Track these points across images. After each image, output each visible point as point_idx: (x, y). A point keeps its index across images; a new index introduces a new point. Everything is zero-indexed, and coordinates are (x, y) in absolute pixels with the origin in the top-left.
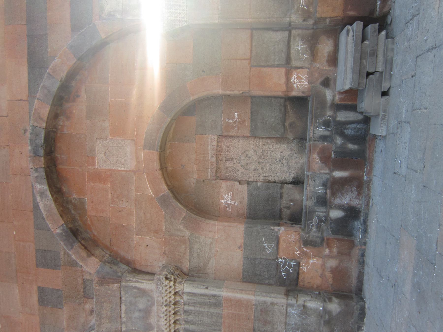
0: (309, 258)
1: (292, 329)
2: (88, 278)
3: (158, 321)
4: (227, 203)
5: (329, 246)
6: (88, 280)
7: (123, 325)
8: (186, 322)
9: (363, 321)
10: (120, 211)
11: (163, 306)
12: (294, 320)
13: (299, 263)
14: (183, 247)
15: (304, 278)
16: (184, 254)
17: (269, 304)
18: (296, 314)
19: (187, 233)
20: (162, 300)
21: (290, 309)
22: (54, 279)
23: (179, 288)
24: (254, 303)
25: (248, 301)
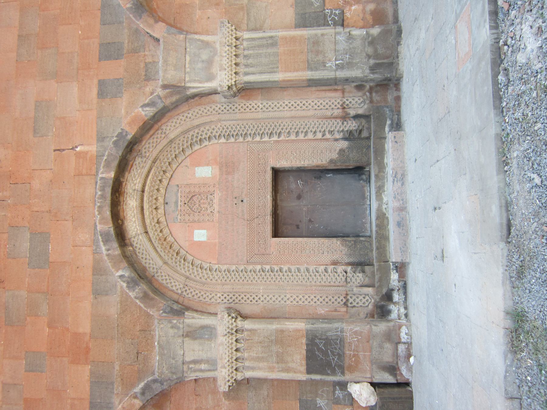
0: (351, 6)
1: (341, 54)
2: (150, 60)
3: (221, 60)
6: (150, 63)
7: (187, 75)
8: (245, 65)
9: (401, 37)
12: (343, 45)
13: (343, 11)
14: (241, 13)
15: (348, 23)
16: (243, 19)
17: (319, 35)
18: (344, 40)
21: (338, 37)
22: (115, 69)
23: (239, 34)
24: (306, 37)
25: (302, 36)
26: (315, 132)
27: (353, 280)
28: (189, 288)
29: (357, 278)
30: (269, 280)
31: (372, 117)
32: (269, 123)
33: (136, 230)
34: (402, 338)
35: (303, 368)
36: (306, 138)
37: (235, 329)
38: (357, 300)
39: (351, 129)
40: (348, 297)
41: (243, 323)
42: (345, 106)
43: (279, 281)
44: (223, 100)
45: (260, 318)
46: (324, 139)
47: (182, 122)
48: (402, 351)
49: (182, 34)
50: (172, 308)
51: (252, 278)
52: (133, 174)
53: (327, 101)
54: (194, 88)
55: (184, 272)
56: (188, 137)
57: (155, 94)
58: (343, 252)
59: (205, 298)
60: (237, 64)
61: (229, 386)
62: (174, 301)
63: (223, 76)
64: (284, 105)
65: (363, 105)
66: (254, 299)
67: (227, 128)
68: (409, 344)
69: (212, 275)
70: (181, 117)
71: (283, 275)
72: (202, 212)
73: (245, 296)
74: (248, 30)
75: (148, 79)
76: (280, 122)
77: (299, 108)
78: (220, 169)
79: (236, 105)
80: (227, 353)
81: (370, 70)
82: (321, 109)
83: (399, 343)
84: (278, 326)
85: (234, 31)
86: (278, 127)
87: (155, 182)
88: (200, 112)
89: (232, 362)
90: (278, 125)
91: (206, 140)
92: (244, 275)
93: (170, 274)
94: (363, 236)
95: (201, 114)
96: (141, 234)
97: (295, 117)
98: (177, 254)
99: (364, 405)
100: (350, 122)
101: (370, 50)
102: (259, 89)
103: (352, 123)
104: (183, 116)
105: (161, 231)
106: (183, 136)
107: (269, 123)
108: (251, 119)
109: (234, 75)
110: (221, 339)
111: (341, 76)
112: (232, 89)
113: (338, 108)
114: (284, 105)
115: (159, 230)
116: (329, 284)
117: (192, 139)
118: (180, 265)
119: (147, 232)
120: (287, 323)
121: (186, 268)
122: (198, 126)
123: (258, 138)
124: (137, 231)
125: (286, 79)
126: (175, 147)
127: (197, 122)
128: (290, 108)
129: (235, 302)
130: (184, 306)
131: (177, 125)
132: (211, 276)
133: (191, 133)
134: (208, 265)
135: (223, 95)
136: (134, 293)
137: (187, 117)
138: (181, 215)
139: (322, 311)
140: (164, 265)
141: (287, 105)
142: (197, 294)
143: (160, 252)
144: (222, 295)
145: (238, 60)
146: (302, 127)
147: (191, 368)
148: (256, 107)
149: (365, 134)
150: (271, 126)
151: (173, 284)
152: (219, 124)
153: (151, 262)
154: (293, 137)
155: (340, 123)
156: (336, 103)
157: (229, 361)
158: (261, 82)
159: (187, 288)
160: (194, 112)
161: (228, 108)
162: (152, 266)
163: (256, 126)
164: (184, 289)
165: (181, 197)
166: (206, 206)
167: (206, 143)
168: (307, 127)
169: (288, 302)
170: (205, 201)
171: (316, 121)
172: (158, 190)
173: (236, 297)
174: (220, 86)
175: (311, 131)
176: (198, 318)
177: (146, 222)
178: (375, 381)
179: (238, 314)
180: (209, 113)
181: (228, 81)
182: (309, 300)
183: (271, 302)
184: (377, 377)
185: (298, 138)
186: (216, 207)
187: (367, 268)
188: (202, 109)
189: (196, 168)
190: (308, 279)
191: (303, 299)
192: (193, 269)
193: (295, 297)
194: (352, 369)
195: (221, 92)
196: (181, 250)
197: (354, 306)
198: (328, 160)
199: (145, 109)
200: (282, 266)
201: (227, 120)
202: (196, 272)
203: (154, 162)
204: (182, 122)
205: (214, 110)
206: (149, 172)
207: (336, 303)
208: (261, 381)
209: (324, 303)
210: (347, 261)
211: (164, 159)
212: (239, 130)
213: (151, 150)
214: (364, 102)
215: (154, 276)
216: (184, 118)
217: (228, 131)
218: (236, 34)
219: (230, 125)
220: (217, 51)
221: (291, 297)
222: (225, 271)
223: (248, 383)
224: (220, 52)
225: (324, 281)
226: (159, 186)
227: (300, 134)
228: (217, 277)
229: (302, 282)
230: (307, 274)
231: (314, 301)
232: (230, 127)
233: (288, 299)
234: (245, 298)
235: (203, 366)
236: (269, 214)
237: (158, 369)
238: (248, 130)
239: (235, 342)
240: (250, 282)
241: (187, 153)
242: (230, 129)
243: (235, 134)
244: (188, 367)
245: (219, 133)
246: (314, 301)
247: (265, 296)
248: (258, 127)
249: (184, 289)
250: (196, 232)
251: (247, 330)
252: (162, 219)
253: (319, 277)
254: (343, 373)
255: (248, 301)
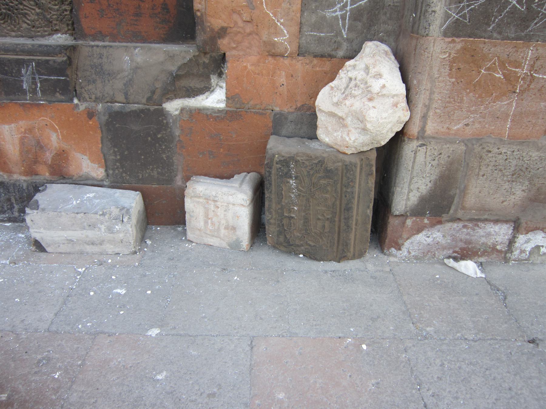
34: (530, 235)
48: (489, 235)
68: (504, 254)
83: (517, 228)
99: (325, 100)
178: (409, 149)
184: (420, 158)
194: (465, 66)
254: (455, 30)
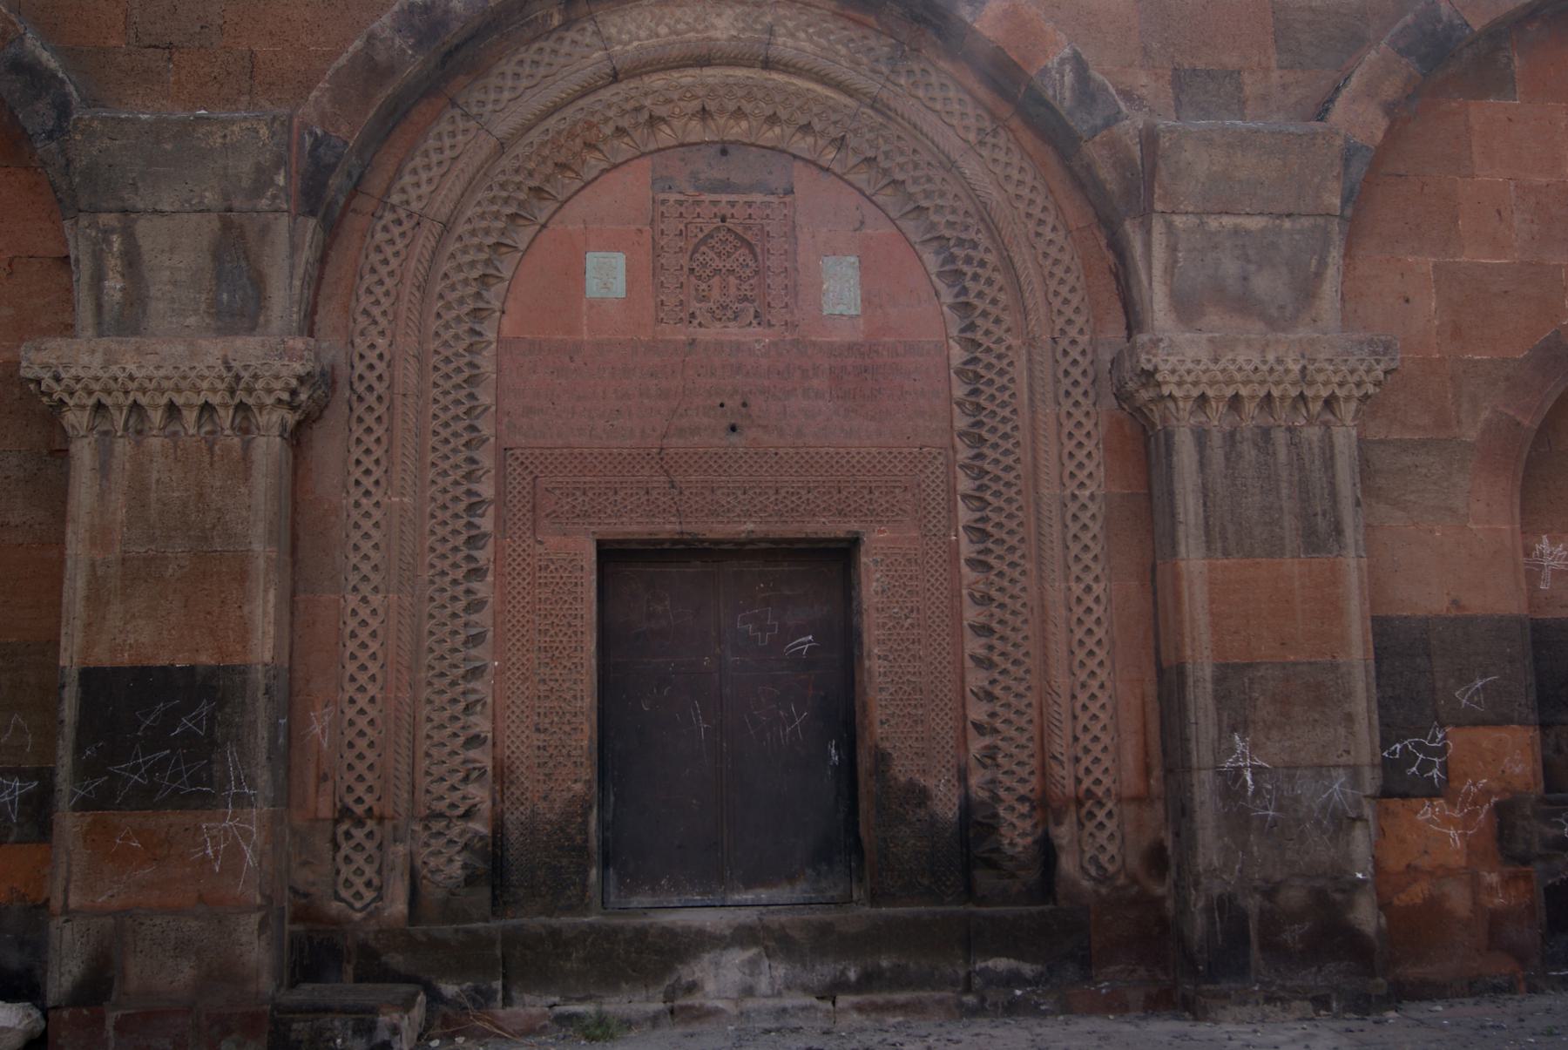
1: (1278, 788)
2: (1248, 90)
3: (1249, 345)
4: (1542, 555)
5: (1507, 882)
8: (1232, 434)
10: (1499, 212)
11: (1303, 362)
18: (1330, 797)
19: (1471, 434)
20: (1322, 356)
21: (1341, 777)
23: (1348, 410)
26: (990, 697)
27: (436, 844)
28: (410, 234)
29: (443, 859)
30: (438, 529)
31: (1050, 906)
32: (1021, 524)
33: (625, 37)
35: (102, 657)
36: (969, 663)
37: (250, 401)
38: (359, 859)
39: (1004, 830)
40: (371, 824)
41: (276, 431)
42: (1089, 804)
43: (432, 566)
44: (1106, 356)
45: (294, 493)
46: (965, 728)
47: (1021, 206)
49: (1345, 201)
50: (331, 168)
51: (445, 465)
52: (832, 26)
53: (1106, 739)
54: (1148, 246)
55: (469, 213)
56: (967, 228)
57: (1122, 104)
58: (542, 806)
59: (369, 291)
60: (1235, 402)
61: (38, 382)
62: (361, 176)
63: (1190, 353)
64: (1088, 579)
65: (1093, 872)
66: (368, 472)
67: (1002, 372)
69: (458, 319)
70: (1040, 200)
71: (455, 582)
72: (692, 279)
73: (378, 440)
74: (1363, 443)
75: (1181, 81)
76: (1028, 566)
77: (1079, 634)
78: (851, 347)
79: (1086, 404)
80: (162, 372)
81: (1220, 896)
82: (1075, 717)
84: (261, 563)
85: (1357, 393)
86: (1009, 558)
87: (799, 108)
88: (1059, 272)
89: (126, 393)
90: (1016, 557)
91: (957, 296)
92: (455, 435)
93: (461, 164)
94: (604, 878)
95: (1052, 275)
96: (610, 58)
97: (1044, 622)
98: (537, 191)
100: (1027, 825)
101: (1294, 896)
102: (1149, 485)
103: (1024, 835)
104: (1045, 209)
105: (620, 131)
106: (972, 210)
107: (1021, 524)
108: (1035, 458)
109: (1195, 393)
110: (214, 350)
111: (1196, 789)
112: (1143, 385)
113: (1078, 781)
114: (1088, 579)
115: (625, 123)
116: (420, 754)
117: (961, 243)
118: (493, 201)
119: (615, 77)
120: (271, 596)
121: (484, 224)
122: (1009, 265)
123: (965, 484)
124: (620, 42)
125: (1185, 584)
126: (929, 180)
127: (1023, 258)
128: (1079, 600)
129: (355, 405)
130: (343, 215)
131: (1011, 188)
132: (454, 313)
133: (983, 239)
134: (496, 304)
135: (1121, 352)
136: (388, 33)
137: (1041, 222)
138: (680, 203)
139: (319, 725)
140: (493, 141)
141: (1088, 589)
142: (386, 262)
143: (541, 128)
144: (381, 357)
145: (1250, 408)
146: (1010, 648)
147: (110, 244)
148: (1082, 475)
149: (984, 879)
150: (1011, 532)
151: (424, 176)
152: (1016, 343)
153: (506, 95)
154: (971, 614)
155: (1022, 790)
156: (1097, 772)
157: (131, 378)
158: (1171, 494)
159: (407, 225)
160: (1062, 249)
161: (1076, 373)
162: (492, 96)
163: (1010, 477)
164: (402, 214)
165: (749, 204)
166: (716, 294)
167: (948, 297)
168: (1009, 666)
169: (353, 601)
170: (733, 290)
171: (1032, 697)
172: (773, 119)
173: (375, 405)
174: (1156, 342)
175: (993, 682)
176: (292, 267)
177: (655, 77)
179: (308, 416)
180: (1057, 303)
181: (1173, 372)
182: (362, 678)
183: (356, 536)
184: (67, 935)
185: (968, 632)
186: (711, 333)
187: (484, 893)
188: (1071, 279)
189: (853, 259)
190: (442, 675)
191: (363, 656)
192: (480, 248)
193: (374, 624)
195: (1133, 347)
196: (553, 206)
197: (336, 847)
198: (886, 745)
199: (1068, 68)
200: (490, 578)
201: (1030, 370)
202: (468, 258)
203: (875, 104)
204: (1021, 206)
205: (1069, 322)
206: (839, 86)
207: (350, 778)
208: (56, 499)
209: (350, 734)
210: (511, 818)
211: (886, 141)
212: (994, 413)
213: (920, 93)
214: (1104, 878)
215: (454, 104)
216: (1036, 211)
217: (989, 375)
218: (1348, 399)
219: (1012, 380)
220: (1284, 330)
221: (374, 612)
222: (472, 365)
223: (52, 453)
224: (1278, 341)
225: (435, 734)
226: (788, 122)
227: (983, 640)
228: (447, 335)
229: (431, 650)
230: (461, 671)
231: (358, 697)
232: (1005, 380)
233: (364, 600)
234: (369, 441)
235: (114, 284)
236: (686, 528)
237: (104, 120)
238: (995, 446)
239: (201, 401)
240: (431, 457)
241: (909, 225)
242: (999, 381)
243: (982, 400)
244: (113, 231)
245: (986, 342)
246: (358, 697)
247: (377, 515)
248: (1008, 485)
249: (402, 214)
250: (619, 260)
251: (247, 446)
252: (665, 136)
253: (447, 714)
255: (357, 453)
